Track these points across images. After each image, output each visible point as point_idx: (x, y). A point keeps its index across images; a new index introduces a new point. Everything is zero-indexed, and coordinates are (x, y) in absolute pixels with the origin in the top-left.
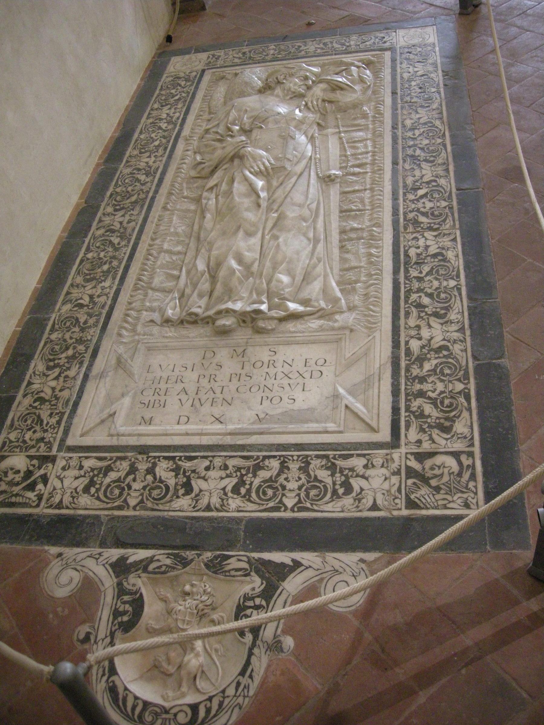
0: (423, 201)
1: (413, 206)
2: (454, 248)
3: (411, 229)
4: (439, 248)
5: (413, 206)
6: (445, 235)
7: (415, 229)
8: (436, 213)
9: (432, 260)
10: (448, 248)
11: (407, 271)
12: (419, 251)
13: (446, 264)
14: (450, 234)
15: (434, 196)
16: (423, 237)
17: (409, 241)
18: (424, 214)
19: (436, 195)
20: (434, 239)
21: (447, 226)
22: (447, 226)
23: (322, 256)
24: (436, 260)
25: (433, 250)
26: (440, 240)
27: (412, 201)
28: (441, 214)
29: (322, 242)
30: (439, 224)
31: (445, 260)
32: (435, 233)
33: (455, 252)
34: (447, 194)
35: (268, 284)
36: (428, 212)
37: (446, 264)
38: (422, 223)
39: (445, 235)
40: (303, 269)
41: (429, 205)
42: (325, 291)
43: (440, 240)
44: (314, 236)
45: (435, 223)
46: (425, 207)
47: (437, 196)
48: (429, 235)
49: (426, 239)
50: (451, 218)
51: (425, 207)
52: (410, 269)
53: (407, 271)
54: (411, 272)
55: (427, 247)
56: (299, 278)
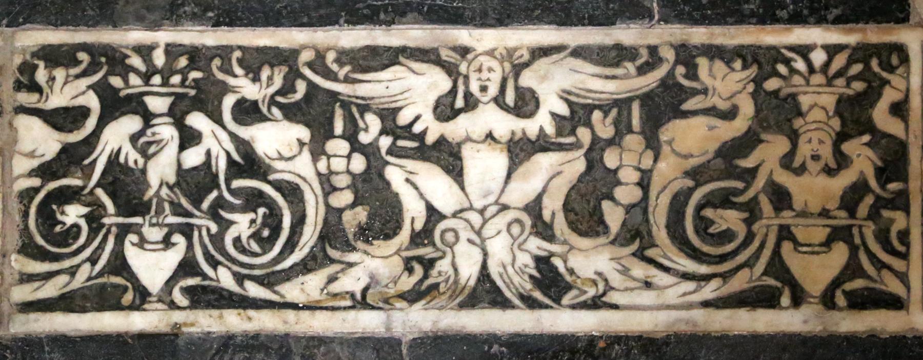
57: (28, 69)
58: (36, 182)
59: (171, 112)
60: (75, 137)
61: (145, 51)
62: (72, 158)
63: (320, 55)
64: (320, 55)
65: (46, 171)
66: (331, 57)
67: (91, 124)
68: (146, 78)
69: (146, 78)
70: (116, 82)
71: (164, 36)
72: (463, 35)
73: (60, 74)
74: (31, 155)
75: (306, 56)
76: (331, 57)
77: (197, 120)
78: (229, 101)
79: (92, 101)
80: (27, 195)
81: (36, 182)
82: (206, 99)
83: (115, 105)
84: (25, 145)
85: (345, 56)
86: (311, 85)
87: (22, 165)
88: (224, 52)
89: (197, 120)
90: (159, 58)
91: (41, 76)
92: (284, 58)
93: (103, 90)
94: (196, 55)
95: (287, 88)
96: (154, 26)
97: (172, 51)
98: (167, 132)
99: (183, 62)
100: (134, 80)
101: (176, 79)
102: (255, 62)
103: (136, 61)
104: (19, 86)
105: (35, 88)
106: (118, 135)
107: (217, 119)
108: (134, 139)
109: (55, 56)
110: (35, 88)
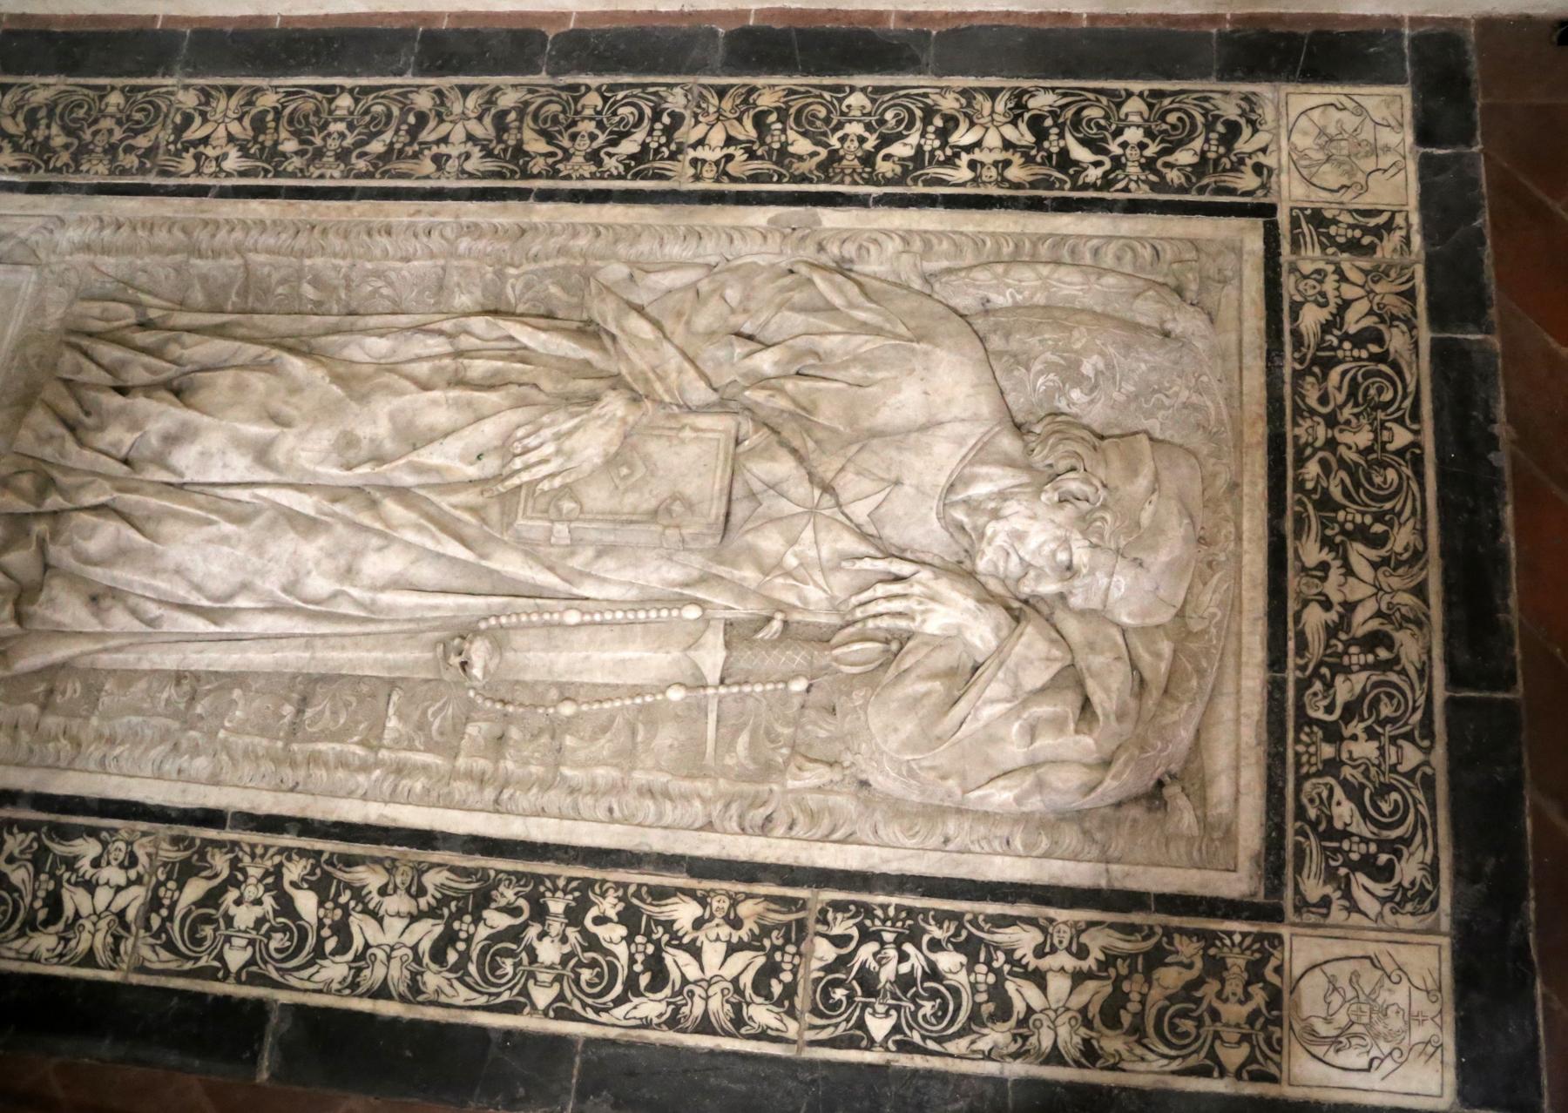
0: (269, 901)
1: (254, 872)
2: (61, 956)
3: (169, 853)
4: (77, 916)
5: (254, 872)
6: (117, 939)
7: (165, 864)
8: (208, 930)
9: (42, 894)
10: (67, 940)
11: (26, 827)
12: (85, 865)
13: (17, 925)
14: (115, 952)
15: (279, 936)
16: (130, 883)
17: (129, 843)
18: (212, 898)
19: (277, 941)
20: (115, 908)
21: (146, 952)
22: (146, 952)
23: (165, 629)
24: (38, 904)
25: (75, 899)
26: (103, 924)
27: (278, 871)
28: (199, 942)
29: (212, 628)
30: (162, 929)
31: (31, 925)
32: (131, 915)
33: (45, 955)
34: (274, 975)
35: (97, 509)
36: (217, 907)
37: (17, 925)
38: (181, 888)
39: (117, 939)
40: (130, 583)
41: (245, 917)
42: (61, 633)
43: (103, 924)
44: (238, 610)
45: (170, 918)
46: (238, 902)
47: (273, 945)
48: (135, 898)
49: (119, 889)
50: (173, 966)
51: (238, 902)
52: (33, 834)
53: (26, 827)
54: (21, 837)
55: (90, 886)
56: (99, 574)
57: (823, 912)
58: (821, 974)
59: (895, 942)
60: (844, 951)
61: (884, 907)
62: (842, 962)
63: (976, 917)
64: (976, 917)
65: (828, 969)
66: (981, 918)
67: (853, 945)
68: (884, 922)
69: (884, 922)
70: (868, 923)
71: (895, 900)
72: (1052, 912)
73: (840, 916)
74: (821, 959)
75: (968, 917)
76: (981, 918)
77: (908, 948)
78: (926, 939)
79: (855, 932)
80: (817, 981)
81: (821, 974)
82: (914, 936)
83: (866, 936)
84: (818, 954)
85: (990, 919)
86: (970, 934)
87: (816, 964)
88: (925, 911)
89: (908, 948)
90: (891, 912)
91: (830, 916)
92: (957, 917)
93: (861, 927)
94: (911, 912)
95: (957, 934)
96: (891, 894)
97: (899, 908)
98: (892, 953)
99: (903, 915)
100: (877, 922)
101: (899, 924)
102: (941, 918)
103: (879, 912)
104: (818, 921)
105: (826, 922)
106: (867, 952)
107: (920, 950)
108: (875, 955)
109: (839, 906)
110: (826, 922)
